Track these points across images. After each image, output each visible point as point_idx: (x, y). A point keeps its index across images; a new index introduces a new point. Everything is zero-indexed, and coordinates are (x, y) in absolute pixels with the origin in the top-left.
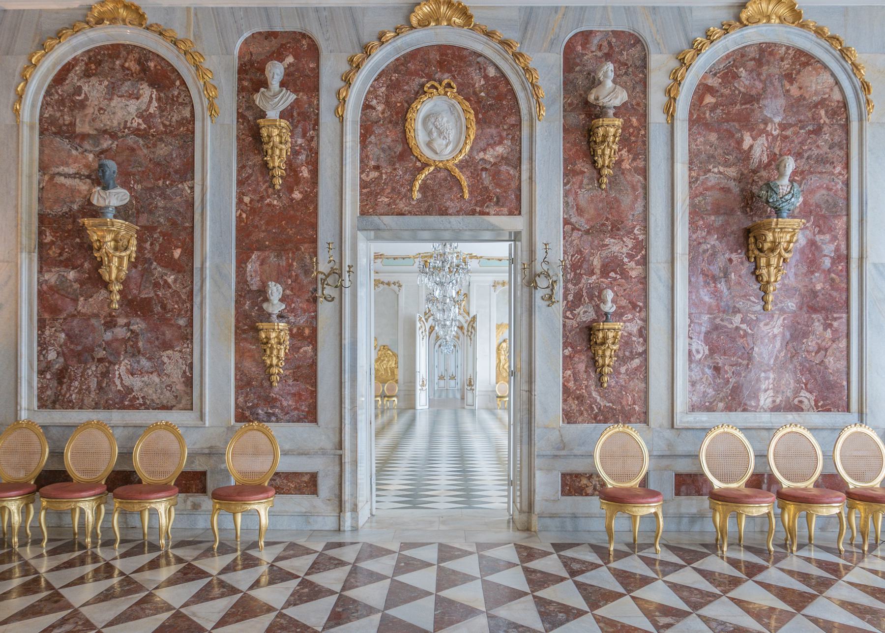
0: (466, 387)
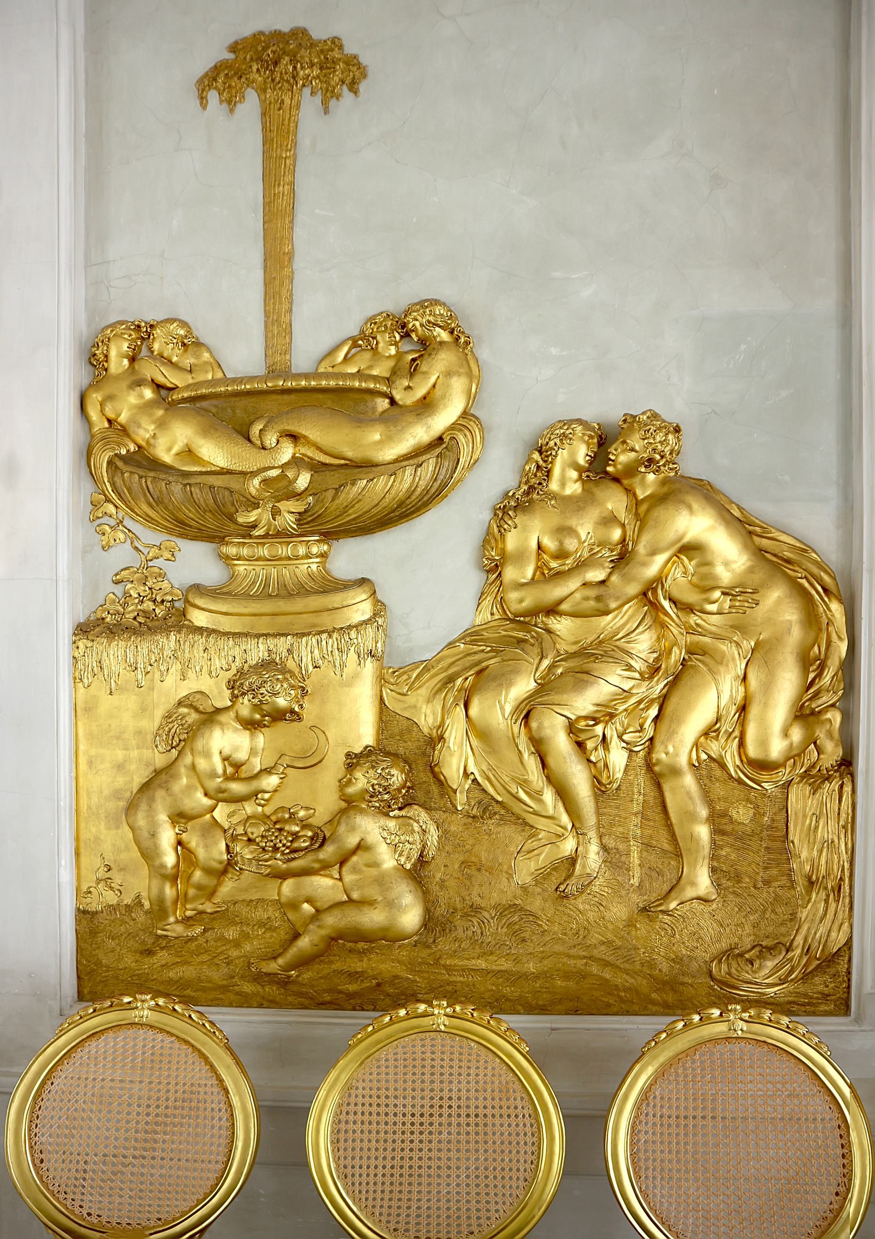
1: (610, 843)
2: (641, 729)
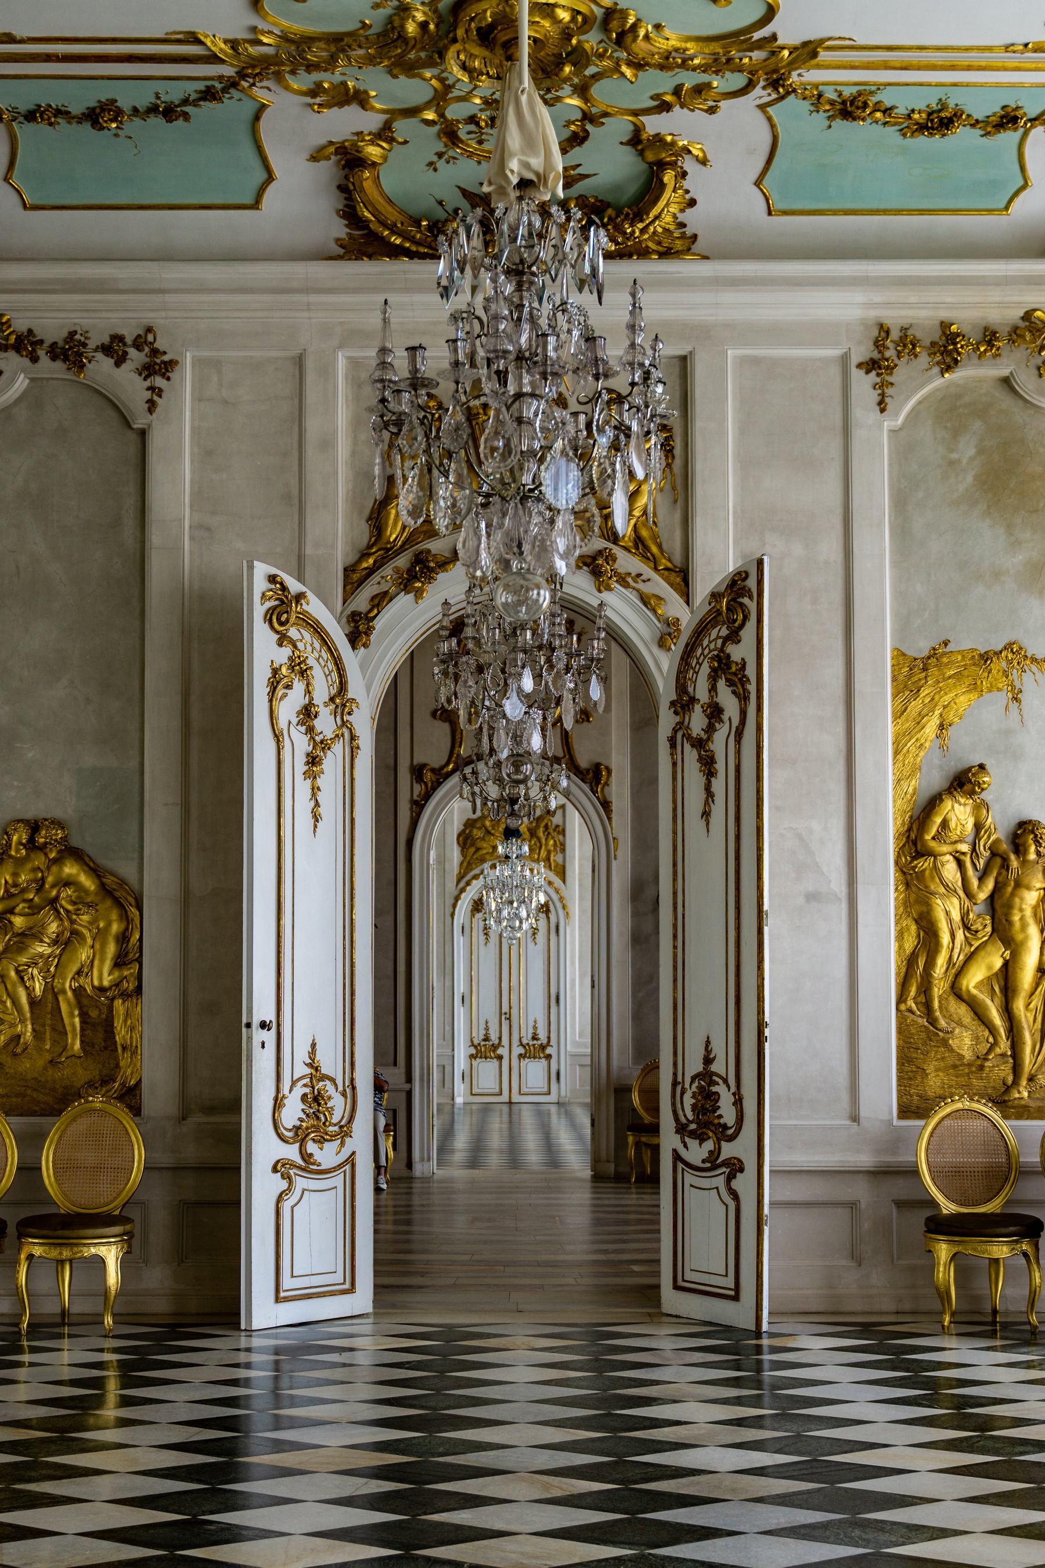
0: (669, 1140)
1: (37, 1028)
2: (48, 970)
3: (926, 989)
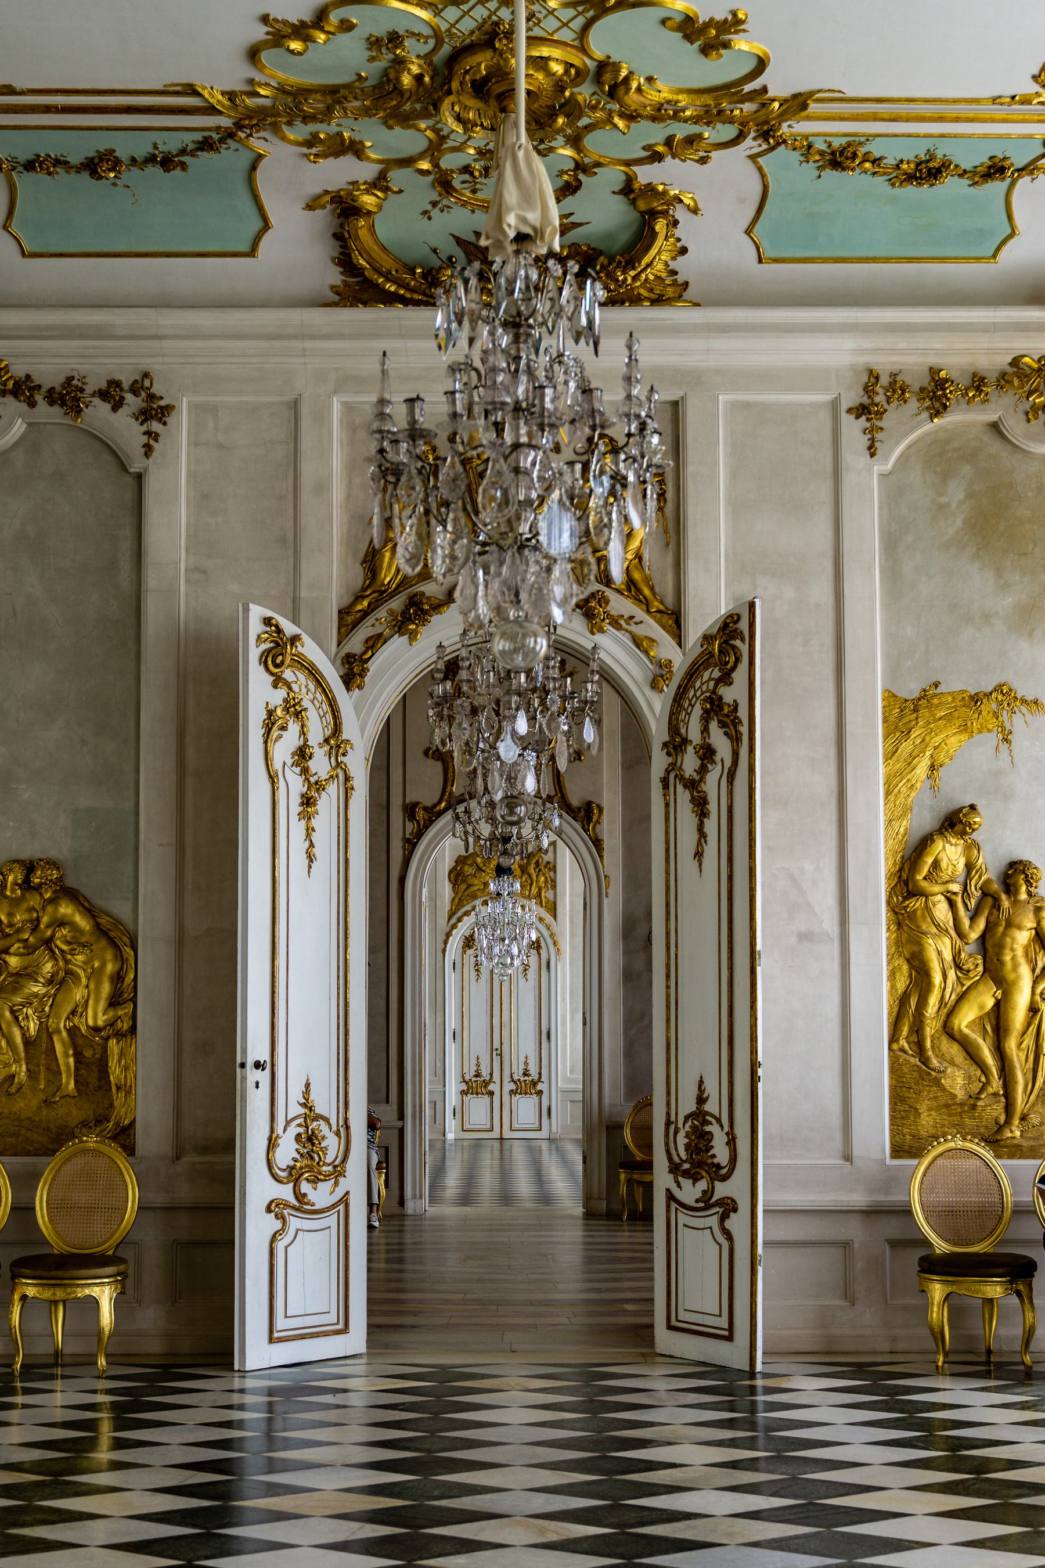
0: (662, 1179)
1: (32, 1067)
2: (43, 1011)
3: (918, 1029)
